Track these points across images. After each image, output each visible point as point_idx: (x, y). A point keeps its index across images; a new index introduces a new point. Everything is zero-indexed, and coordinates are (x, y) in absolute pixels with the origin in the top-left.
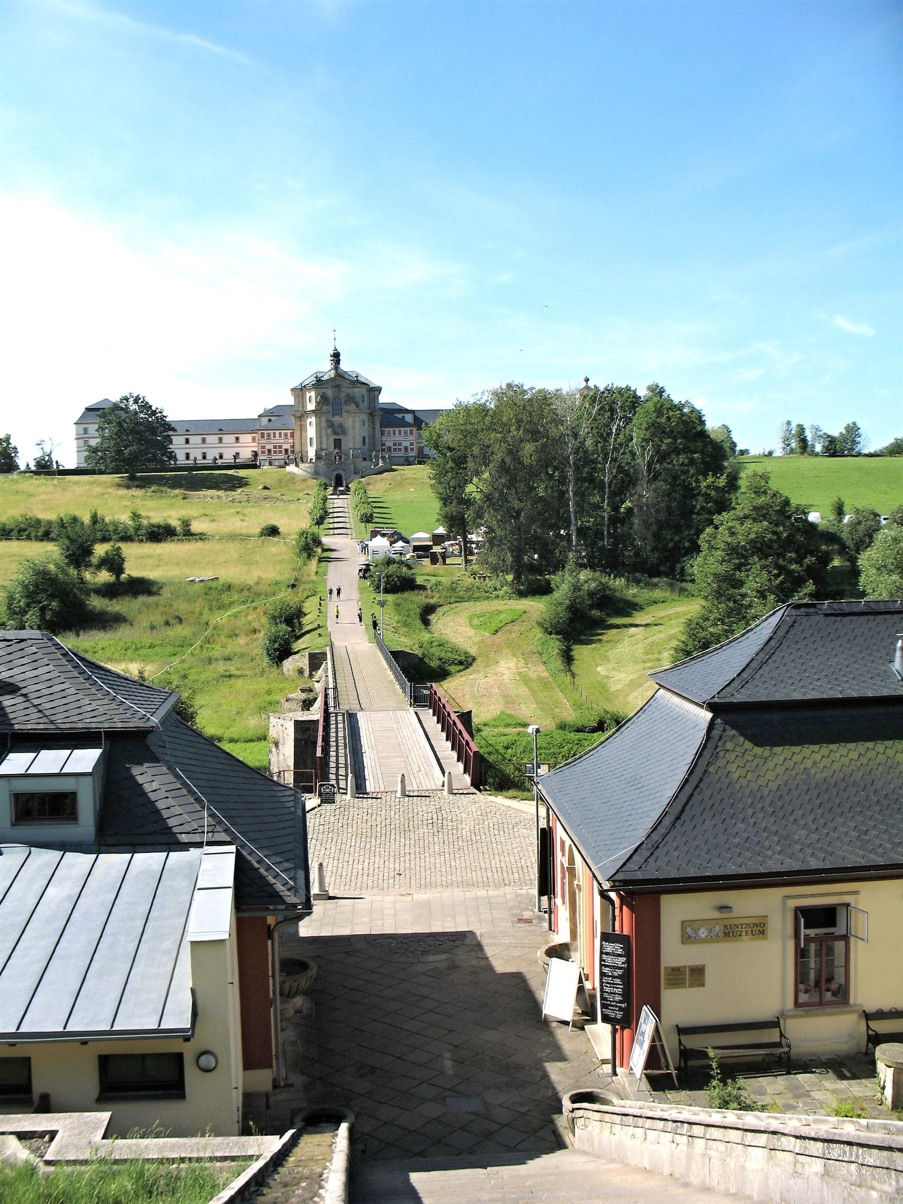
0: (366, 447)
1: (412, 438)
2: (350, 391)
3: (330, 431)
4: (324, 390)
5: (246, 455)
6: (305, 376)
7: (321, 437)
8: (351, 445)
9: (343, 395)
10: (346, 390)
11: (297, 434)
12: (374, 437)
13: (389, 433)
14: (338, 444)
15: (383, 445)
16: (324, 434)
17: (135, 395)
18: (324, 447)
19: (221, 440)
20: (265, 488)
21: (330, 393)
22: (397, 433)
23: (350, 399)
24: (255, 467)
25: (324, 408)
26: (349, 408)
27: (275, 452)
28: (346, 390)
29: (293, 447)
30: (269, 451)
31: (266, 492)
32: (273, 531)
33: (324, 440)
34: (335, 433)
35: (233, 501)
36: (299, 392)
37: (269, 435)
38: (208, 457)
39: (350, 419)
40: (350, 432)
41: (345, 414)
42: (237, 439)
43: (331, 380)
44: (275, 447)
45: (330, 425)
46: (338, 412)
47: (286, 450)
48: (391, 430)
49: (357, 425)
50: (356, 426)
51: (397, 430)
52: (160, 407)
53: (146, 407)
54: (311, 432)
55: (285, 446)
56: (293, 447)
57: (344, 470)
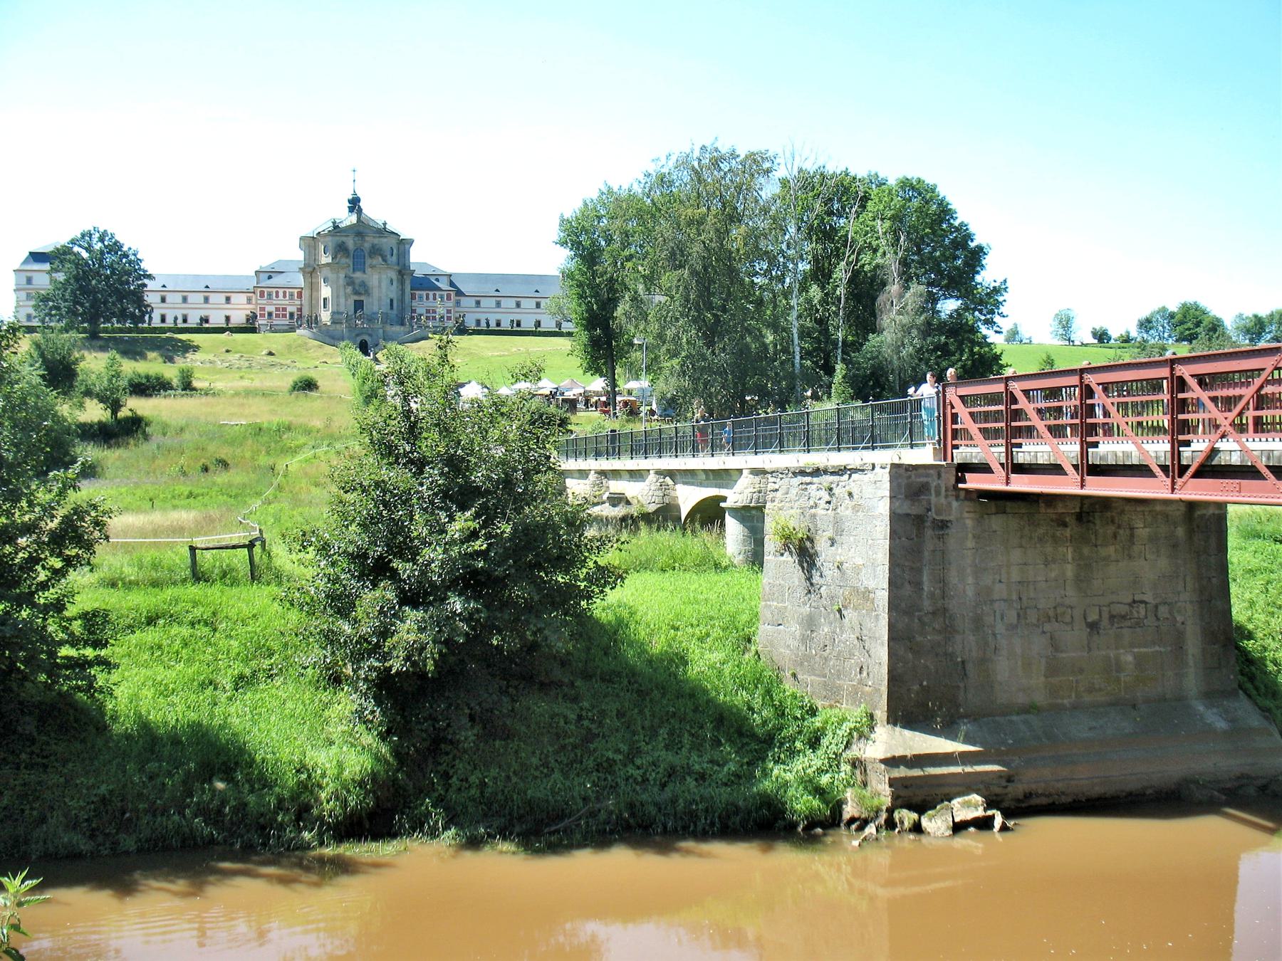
0: (395, 312)
1: (450, 304)
2: (376, 241)
3: (349, 289)
4: (344, 239)
5: (239, 318)
6: (319, 222)
7: (338, 297)
8: (375, 309)
9: (367, 246)
10: (370, 240)
11: (306, 294)
12: (402, 301)
13: (421, 297)
14: (359, 305)
15: (414, 311)
16: (342, 293)
17: (101, 230)
18: (342, 309)
19: (206, 300)
20: (271, 354)
21: (350, 243)
22: (431, 297)
23: (376, 251)
24: (253, 330)
25: (344, 260)
26: (374, 262)
27: (277, 316)
28: (370, 240)
29: (300, 310)
30: (270, 314)
31: (271, 358)
32: (308, 385)
33: (342, 300)
34: (356, 293)
35: (230, 367)
36: (310, 243)
37: (270, 294)
38: (189, 320)
39: (376, 277)
40: (375, 293)
41: (368, 270)
42: (228, 299)
43: (351, 227)
44: (277, 309)
45: (350, 282)
46: (359, 264)
47: (292, 315)
48: (424, 293)
49: (385, 283)
50: (381, 283)
51: (431, 294)
52: (134, 248)
53: (115, 247)
54: (326, 292)
55: (290, 309)
56: (300, 310)
57: (370, 335)
